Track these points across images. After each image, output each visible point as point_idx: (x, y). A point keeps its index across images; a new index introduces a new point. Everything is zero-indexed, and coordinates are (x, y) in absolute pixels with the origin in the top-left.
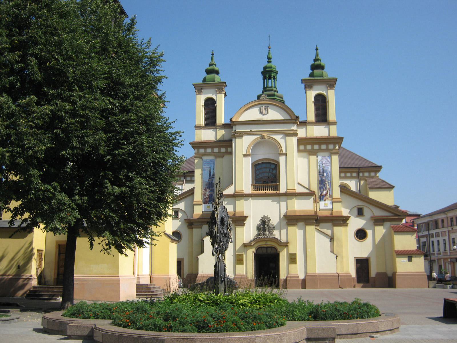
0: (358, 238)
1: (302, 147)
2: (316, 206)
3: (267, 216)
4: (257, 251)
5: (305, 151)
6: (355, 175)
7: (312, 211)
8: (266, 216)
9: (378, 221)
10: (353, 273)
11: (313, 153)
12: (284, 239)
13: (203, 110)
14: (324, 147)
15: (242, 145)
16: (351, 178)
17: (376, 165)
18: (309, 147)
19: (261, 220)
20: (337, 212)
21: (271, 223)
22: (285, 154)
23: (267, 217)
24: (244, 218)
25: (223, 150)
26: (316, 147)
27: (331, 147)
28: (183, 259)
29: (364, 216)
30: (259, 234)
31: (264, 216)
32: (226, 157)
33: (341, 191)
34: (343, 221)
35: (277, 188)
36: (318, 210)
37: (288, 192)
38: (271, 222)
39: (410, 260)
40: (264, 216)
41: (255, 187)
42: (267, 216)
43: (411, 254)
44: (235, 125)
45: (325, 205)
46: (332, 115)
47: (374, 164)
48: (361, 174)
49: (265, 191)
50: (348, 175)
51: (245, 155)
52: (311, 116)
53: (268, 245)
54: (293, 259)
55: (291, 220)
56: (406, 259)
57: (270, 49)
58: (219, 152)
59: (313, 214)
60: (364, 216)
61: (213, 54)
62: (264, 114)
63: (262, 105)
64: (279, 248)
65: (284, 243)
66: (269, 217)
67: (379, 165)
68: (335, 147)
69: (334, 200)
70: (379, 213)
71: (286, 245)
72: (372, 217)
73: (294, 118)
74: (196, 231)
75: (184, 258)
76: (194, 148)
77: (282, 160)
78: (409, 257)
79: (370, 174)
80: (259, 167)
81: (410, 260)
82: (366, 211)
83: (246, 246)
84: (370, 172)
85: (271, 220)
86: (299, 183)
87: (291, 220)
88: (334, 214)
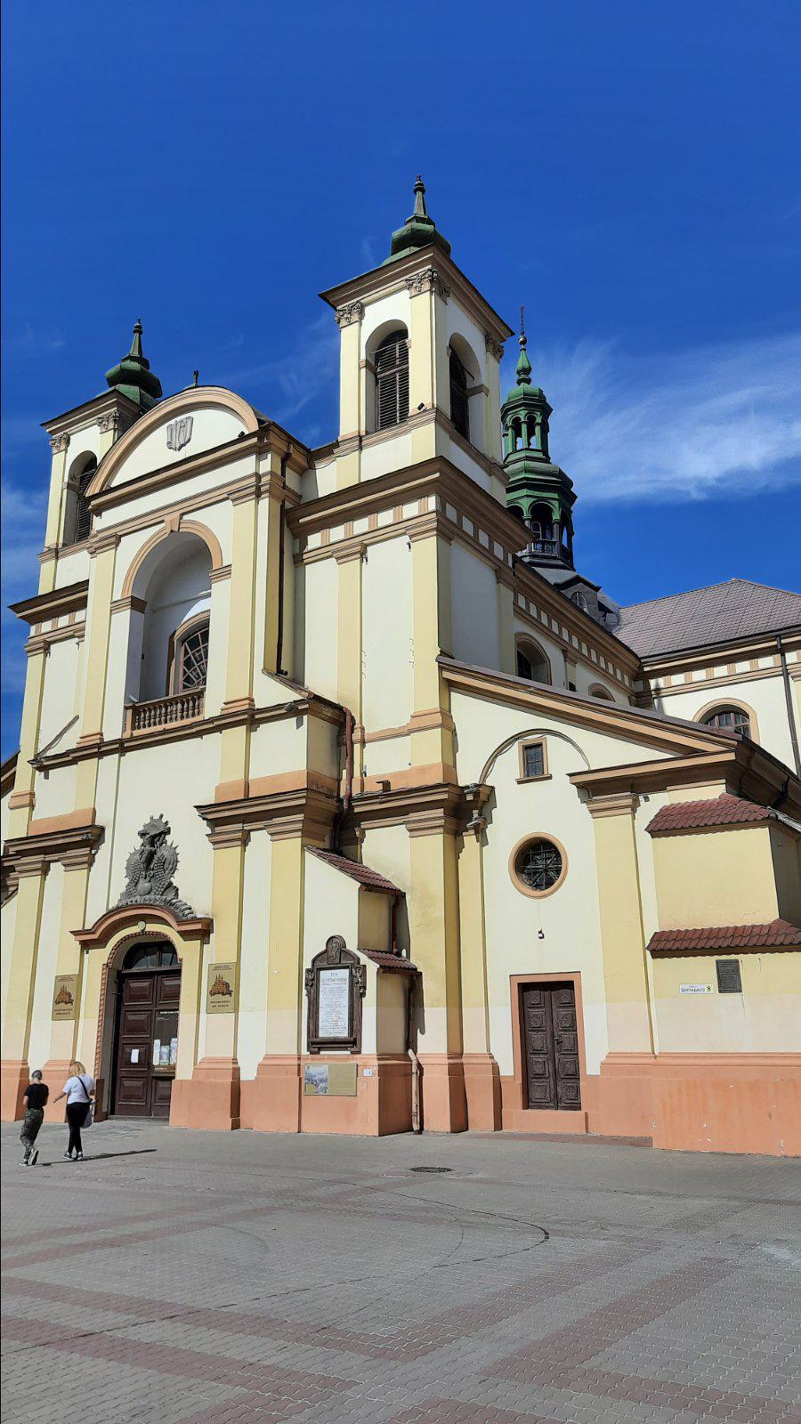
3: (161, 816)
14: (385, 518)
18: (337, 533)
19: (142, 835)
20: (423, 770)
21: (169, 844)
22: (226, 572)
26: (361, 525)
27: (410, 510)
30: (128, 894)
31: (152, 818)
34: (464, 810)
37: (225, 712)
38: (167, 837)
39: (729, 981)
40: (152, 818)
42: (161, 816)
54: (223, 990)
55: (232, 818)
60: (550, 778)
63: (172, 422)
64: (186, 950)
65: (195, 920)
66: (164, 820)
71: (203, 931)
72: (570, 775)
73: (255, 427)
81: (729, 981)
85: (168, 832)
87: (232, 818)
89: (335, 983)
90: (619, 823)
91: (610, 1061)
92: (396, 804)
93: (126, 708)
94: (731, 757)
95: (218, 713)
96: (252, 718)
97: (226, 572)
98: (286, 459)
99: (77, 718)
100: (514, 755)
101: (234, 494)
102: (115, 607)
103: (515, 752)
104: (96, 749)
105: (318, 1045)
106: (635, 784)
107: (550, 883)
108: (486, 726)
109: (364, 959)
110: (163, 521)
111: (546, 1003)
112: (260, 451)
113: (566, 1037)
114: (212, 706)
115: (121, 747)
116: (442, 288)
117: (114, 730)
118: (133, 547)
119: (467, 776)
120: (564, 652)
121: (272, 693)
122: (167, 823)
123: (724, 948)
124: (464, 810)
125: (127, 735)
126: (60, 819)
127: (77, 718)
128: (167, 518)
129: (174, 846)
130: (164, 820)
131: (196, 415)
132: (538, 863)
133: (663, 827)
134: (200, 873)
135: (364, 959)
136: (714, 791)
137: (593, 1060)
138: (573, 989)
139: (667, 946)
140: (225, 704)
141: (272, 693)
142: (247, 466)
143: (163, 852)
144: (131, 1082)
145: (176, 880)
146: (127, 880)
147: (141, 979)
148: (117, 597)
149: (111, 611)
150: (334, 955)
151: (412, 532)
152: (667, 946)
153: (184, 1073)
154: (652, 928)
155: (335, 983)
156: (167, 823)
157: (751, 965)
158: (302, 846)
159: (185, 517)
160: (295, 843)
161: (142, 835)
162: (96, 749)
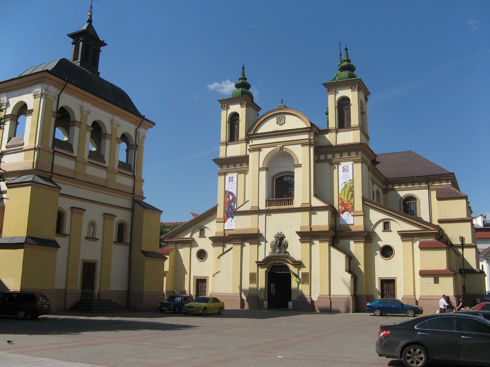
0: (383, 256)
1: (322, 157)
2: (336, 221)
3: (281, 232)
4: (271, 270)
7: (325, 226)
8: (280, 232)
9: (405, 236)
17: (448, 172)
22: (299, 166)
23: (279, 234)
25: (245, 166)
28: (208, 277)
29: (391, 231)
33: (363, 203)
36: (338, 225)
37: (302, 206)
39: (436, 281)
41: (269, 202)
42: (281, 232)
43: (437, 275)
46: (355, 120)
47: (447, 171)
49: (280, 206)
52: (333, 123)
53: (281, 263)
56: (432, 279)
57: (341, 55)
59: (327, 229)
60: (391, 231)
61: (243, 68)
62: (280, 125)
66: (282, 234)
67: (451, 172)
68: (357, 154)
69: (356, 214)
71: (299, 264)
72: (398, 232)
74: (220, 250)
75: (208, 277)
76: (218, 164)
78: (434, 277)
81: (436, 281)
82: (392, 224)
83: (260, 264)
84: (440, 181)
86: (316, 196)
91: (403, 297)
93: (266, 200)
94: (437, 231)
95: (299, 206)
96: (312, 210)
97: (299, 166)
98: (315, 134)
99: (248, 201)
100: (381, 225)
102: (260, 169)
108: (375, 216)
110: (276, 146)
111: (389, 284)
112: (309, 132)
113: (392, 292)
116: (359, 90)
117: (263, 207)
118: (265, 152)
120: (372, 181)
121: (316, 203)
122: (283, 234)
123: (436, 275)
125: (267, 208)
127: (248, 201)
128: (277, 146)
129: (286, 241)
130: (282, 234)
131: (287, 117)
132: (387, 252)
133: (423, 247)
136: (431, 240)
138: (394, 283)
139: (424, 274)
140: (302, 204)
141: (316, 203)
142: (306, 136)
143: (283, 242)
145: (288, 250)
146: (271, 249)
148: (261, 166)
149: (259, 170)
152: (424, 274)
154: (418, 269)
156: (283, 234)
157: (441, 279)
158: (329, 245)
159: (285, 147)
160: (326, 244)
161: (275, 237)
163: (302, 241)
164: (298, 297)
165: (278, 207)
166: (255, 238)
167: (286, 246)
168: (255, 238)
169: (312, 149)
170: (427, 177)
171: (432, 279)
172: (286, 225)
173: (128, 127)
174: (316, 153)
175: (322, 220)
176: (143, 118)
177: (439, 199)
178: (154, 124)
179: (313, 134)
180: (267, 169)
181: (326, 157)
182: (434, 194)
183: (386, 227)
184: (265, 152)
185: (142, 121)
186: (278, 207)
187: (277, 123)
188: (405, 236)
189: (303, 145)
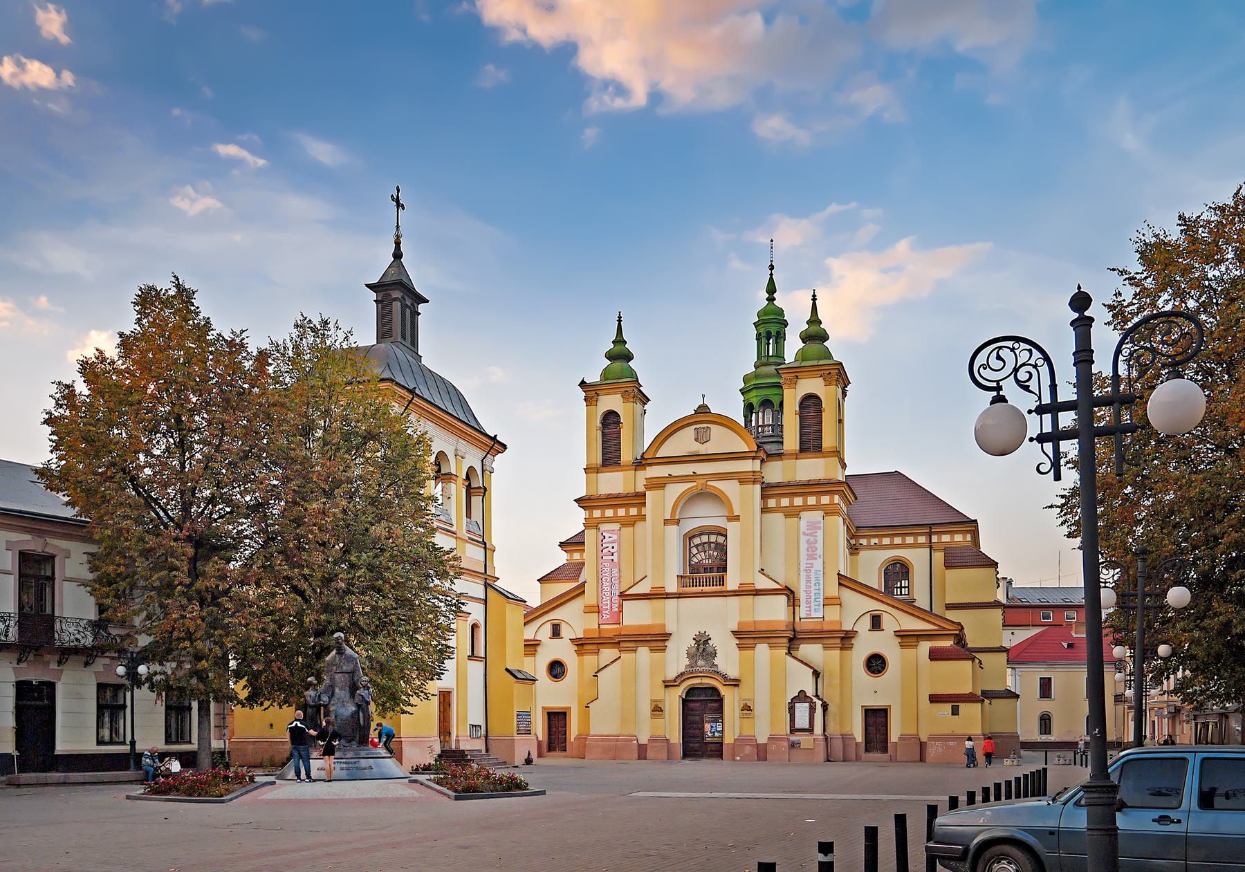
1: (772, 503)
5: (777, 509)
6: (922, 539)
9: (907, 638)
10: (859, 737)
11: (792, 513)
12: (733, 673)
13: (599, 434)
14: (812, 500)
15: (660, 504)
16: (915, 545)
18: (785, 502)
20: (831, 622)
23: (701, 635)
24: (665, 637)
25: (633, 511)
26: (798, 501)
30: (690, 666)
32: (639, 525)
34: (846, 639)
35: (722, 581)
36: (797, 619)
39: (955, 711)
44: (650, 465)
45: (811, 612)
46: (828, 441)
48: (935, 539)
50: (910, 540)
51: (666, 522)
54: (747, 708)
55: (746, 637)
56: (948, 708)
58: (627, 515)
64: (724, 691)
70: (912, 624)
71: (736, 683)
77: (732, 529)
79: (952, 538)
80: (697, 541)
81: (955, 711)
82: (886, 621)
87: (746, 637)
88: (826, 628)
89: (802, 710)
90: (910, 652)
92: (818, 636)
95: (736, 588)
101: (742, 478)
102: (666, 522)
103: (868, 618)
104: (658, 595)
105: (793, 730)
106: (918, 636)
107: (879, 672)
109: (815, 699)
112: (754, 458)
114: (732, 583)
115: (679, 596)
119: (848, 627)
123: (955, 701)
124: (846, 639)
126: (641, 626)
132: (876, 664)
134: (728, 659)
135: (815, 699)
137: (894, 736)
139: (934, 699)
144: (697, 745)
145: (716, 661)
147: (701, 703)
150: (802, 697)
151: (829, 511)
152: (934, 699)
153: (728, 740)
155: (802, 710)
157: (963, 707)
162: (658, 595)
163: (740, 647)
164: (736, 740)
165: (699, 589)
166: (658, 639)
167: (714, 655)
168: (658, 639)
169: (758, 487)
170: (930, 526)
171: (948, 708)
172: (716, 617)
173: (473, 458)
174: (764, 497)
175: (774, 611)
176: (494, 438)
177: (948, 566)
178: (504, 447)
179: (758, 462)
180: (678, 522)
181: (778, 503)
182: (939, 557)
183: (876, 623)
184: (674, 491)
185: (495, 446)
186: (699, 589)
187: (696, 440)
188: (907, 638)
189: (742, 481)
